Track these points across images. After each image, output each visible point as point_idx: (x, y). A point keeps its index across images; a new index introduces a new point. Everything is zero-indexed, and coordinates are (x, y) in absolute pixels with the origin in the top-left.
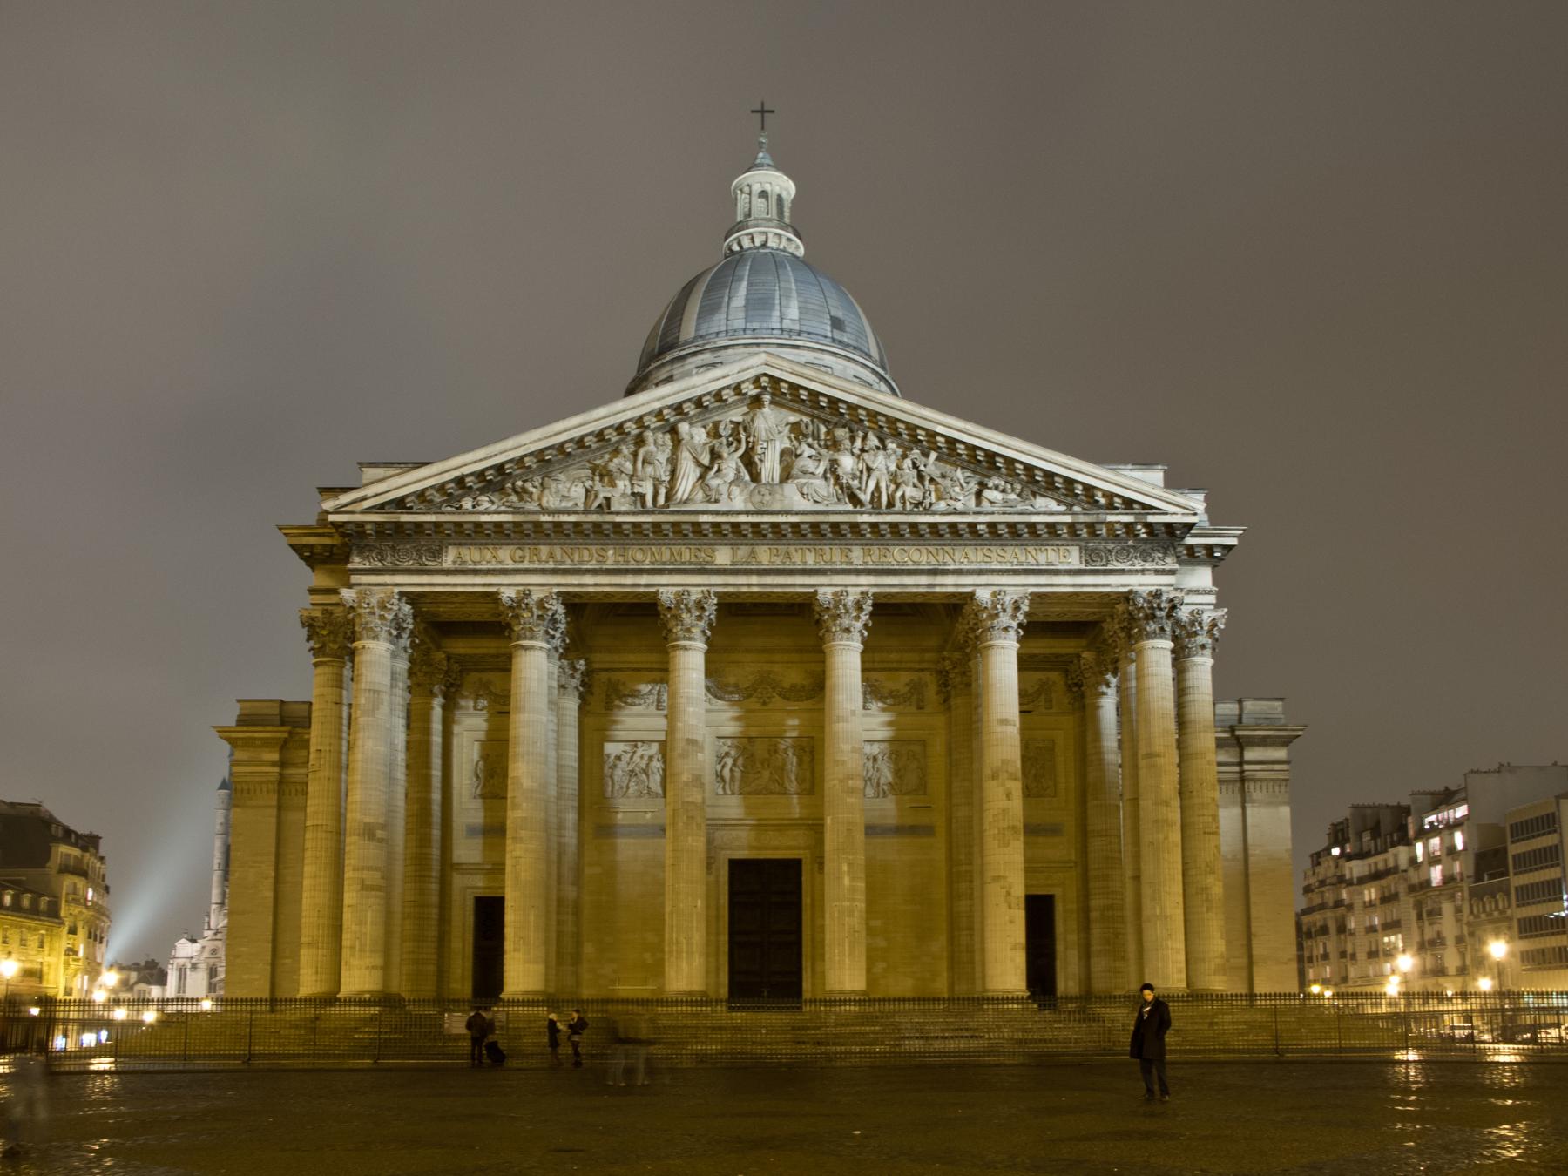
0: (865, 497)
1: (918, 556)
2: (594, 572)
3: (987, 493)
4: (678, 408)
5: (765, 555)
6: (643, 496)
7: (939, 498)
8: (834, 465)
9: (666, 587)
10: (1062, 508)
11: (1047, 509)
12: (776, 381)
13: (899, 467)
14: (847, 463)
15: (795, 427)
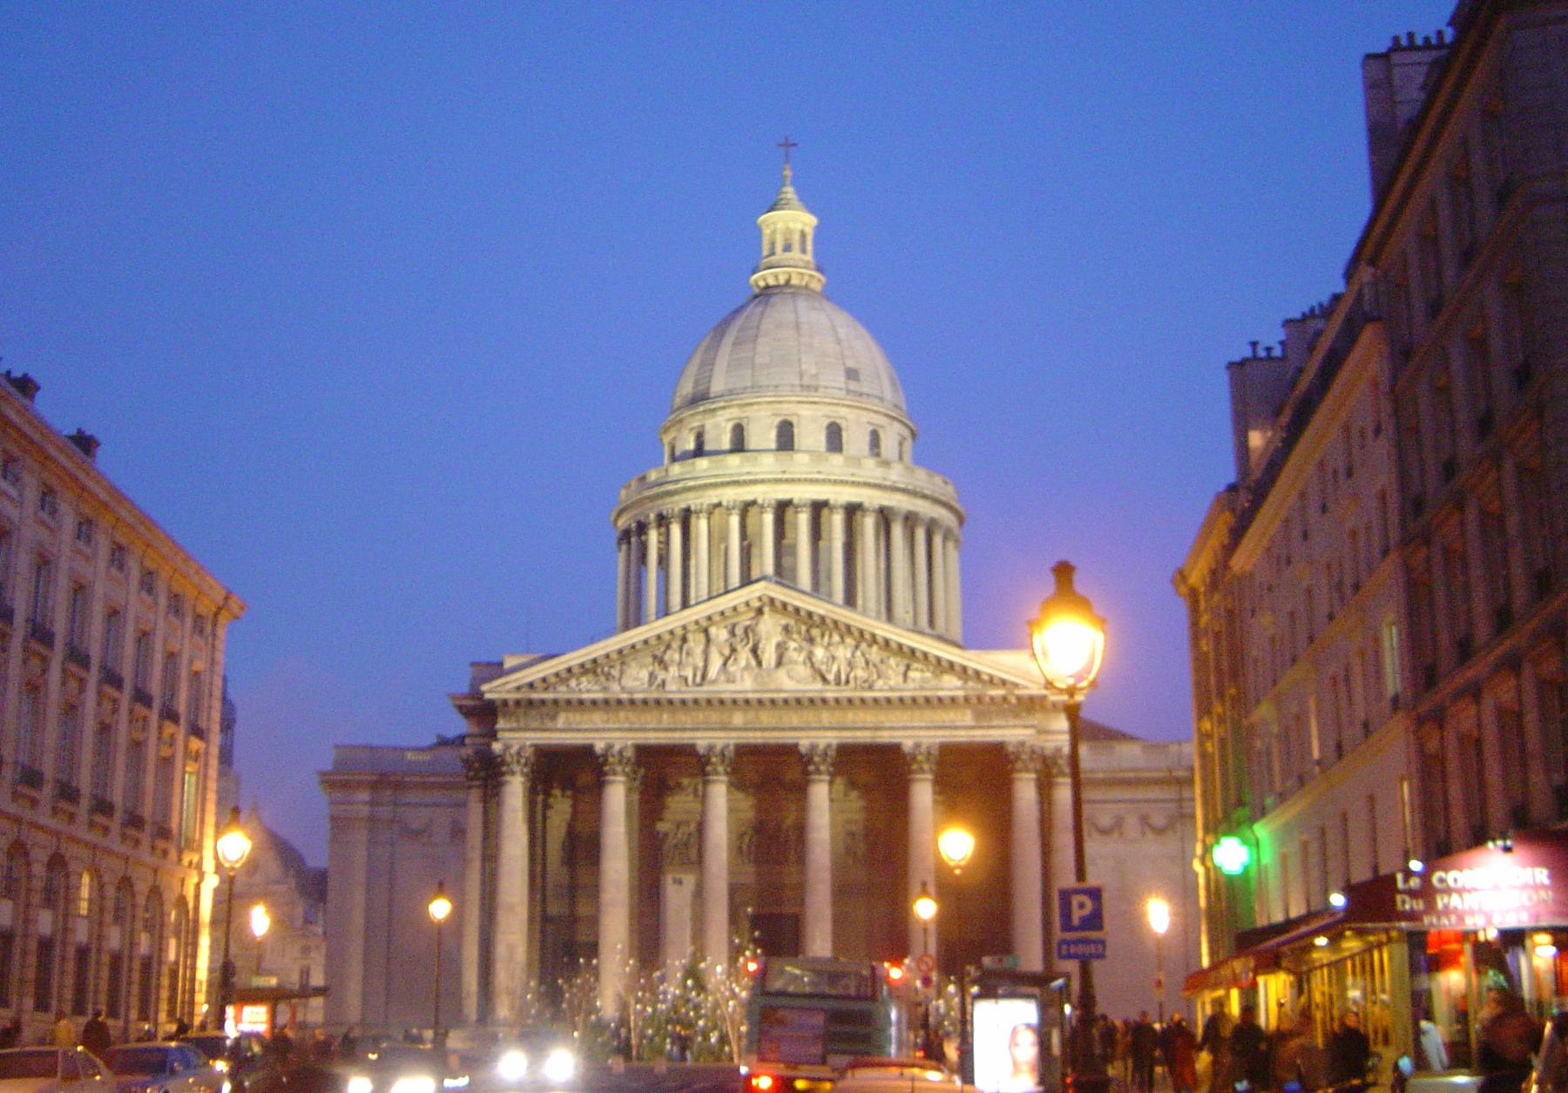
0: (831, 677)
1: (867, 717)
2: (655, 730)
3: (912, 674)
4: (709, 618)
5: (766, 718)
6: (686, 679)
7: (879, 677)
8: (810, 656)
9: (702, 740)
10: (959, 683)
11: (950, 685)
12: (772, 601)
13: (853, 655)
14: (819, 653)
15: (786, 629)
